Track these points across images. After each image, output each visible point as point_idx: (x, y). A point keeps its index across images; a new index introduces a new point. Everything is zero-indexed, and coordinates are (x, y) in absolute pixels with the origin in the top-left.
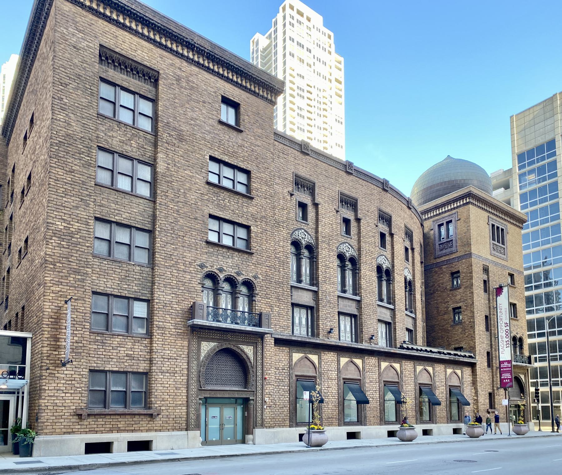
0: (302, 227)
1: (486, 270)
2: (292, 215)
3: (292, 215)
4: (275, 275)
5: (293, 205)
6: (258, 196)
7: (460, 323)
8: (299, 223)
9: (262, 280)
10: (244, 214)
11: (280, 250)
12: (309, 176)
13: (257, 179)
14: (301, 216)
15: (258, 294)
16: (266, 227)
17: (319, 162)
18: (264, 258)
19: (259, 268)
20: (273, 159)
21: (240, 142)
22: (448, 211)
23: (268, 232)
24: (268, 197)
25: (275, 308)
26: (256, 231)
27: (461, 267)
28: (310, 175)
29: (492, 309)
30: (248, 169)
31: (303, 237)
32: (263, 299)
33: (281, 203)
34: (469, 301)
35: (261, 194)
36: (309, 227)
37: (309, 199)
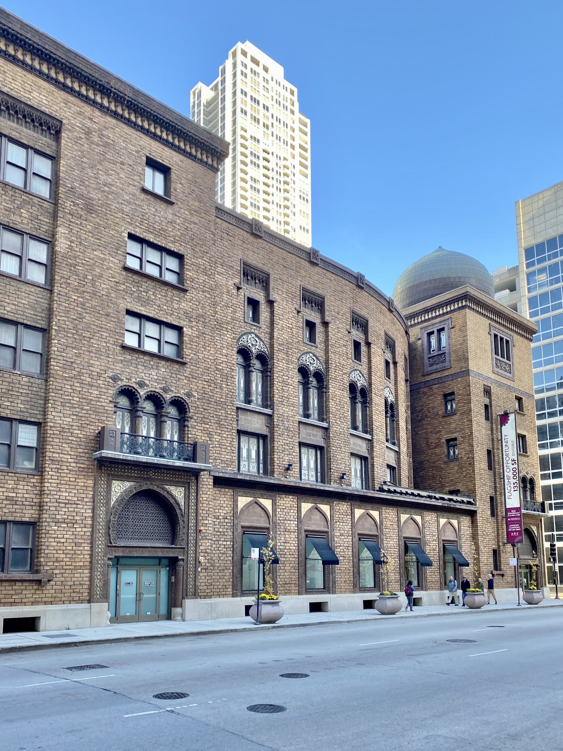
0: (253, 331)
1: (487, 392)
2: (239, 314)
3: (239, 315)
4: (215, 392)
5: (241, 302)
6: (194, 288)
7: (456, 458)
8: (248, 325)
9: (198, 399)
10: (175, 310)
11: (222, 359)
12: (261, 265)
13: (192, 266)
14: (251, 316)
15: (191, 418)
16: (205, 329)
17: (275, 248)
18: (201, 370)
19: (193, 383)
20: (215, 241)
21: (170, 216)
23: (207, 336)
24: (207, 289)
25: (215, 437)
26: (190, 334)
28: (263, 264)
30: (180, 252)
31: (254, 343)
32: (198, 424)
33: (224, 298)
34: (467, 431)
35: (198, 286)
36: (261, 330)
37: (262, 294)
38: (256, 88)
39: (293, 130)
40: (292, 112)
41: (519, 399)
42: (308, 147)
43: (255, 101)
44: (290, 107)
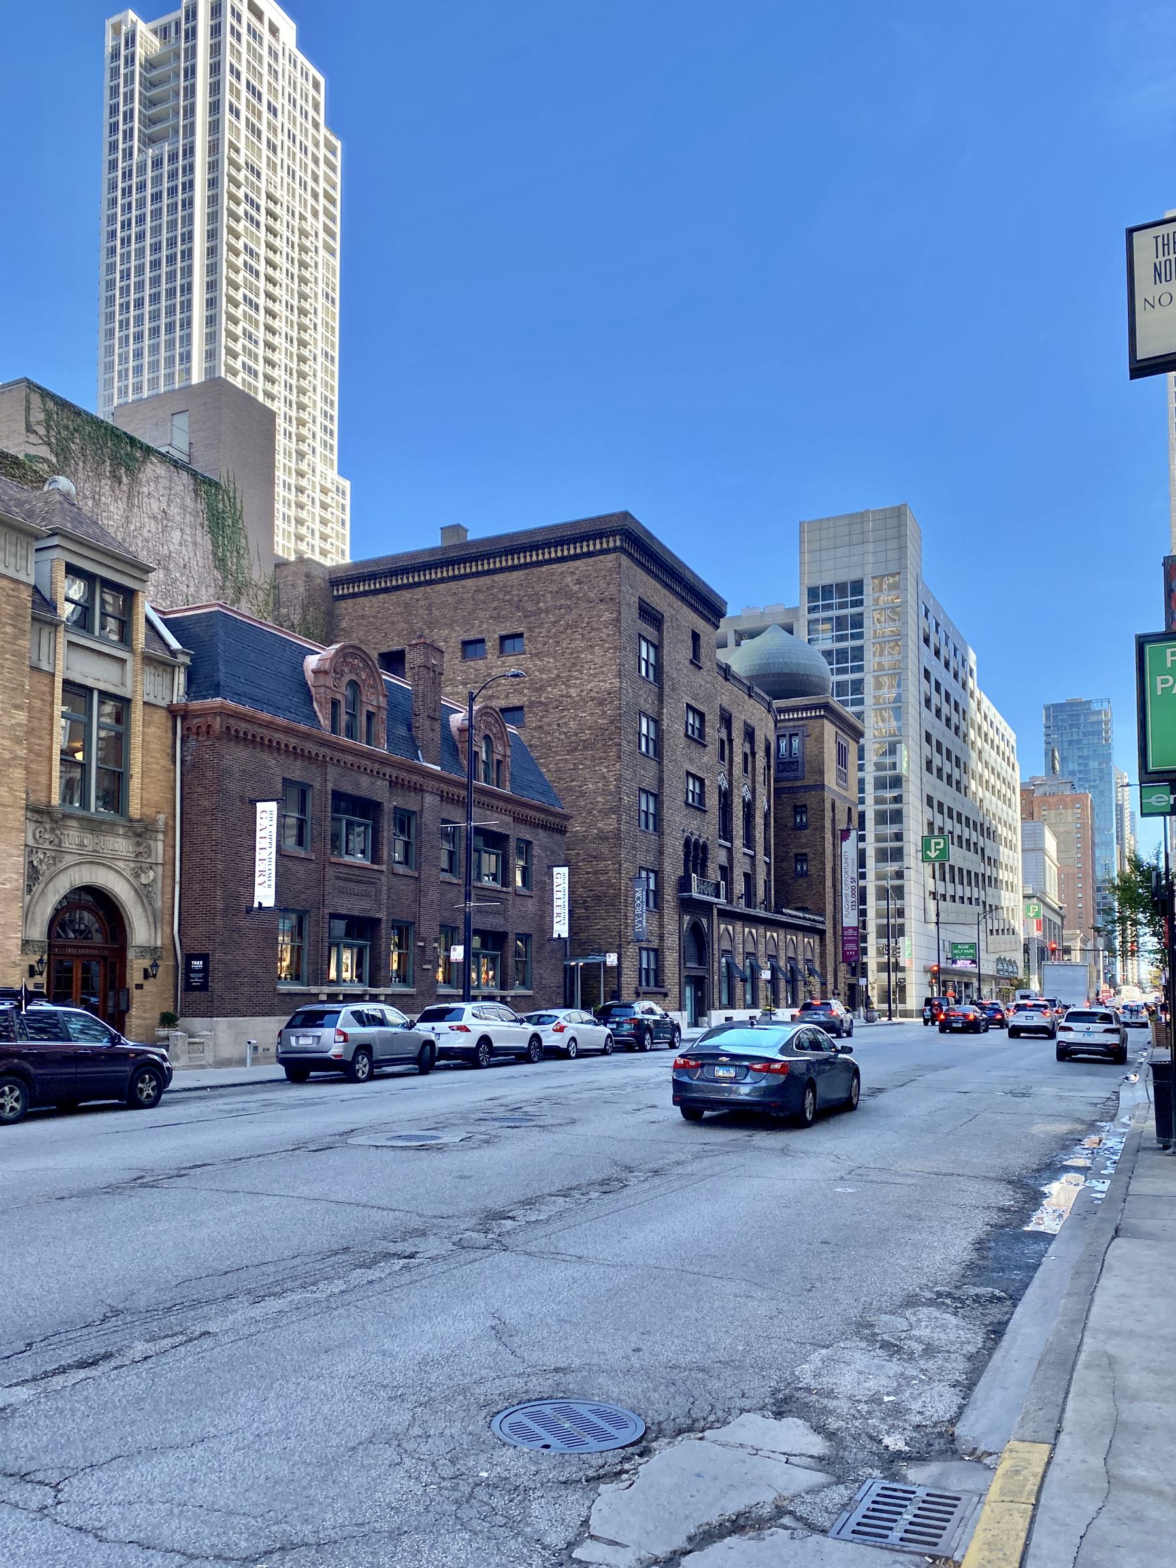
7: (805, 875)
22: (794, 719)
27: (810, 799)
29: (837, 857)
38: (256, 65)
39: (316, 161)
40: (316, 125)
41: (850, 809)
42: (337, 196)
43: (254, 94)
44: (311, 113)
